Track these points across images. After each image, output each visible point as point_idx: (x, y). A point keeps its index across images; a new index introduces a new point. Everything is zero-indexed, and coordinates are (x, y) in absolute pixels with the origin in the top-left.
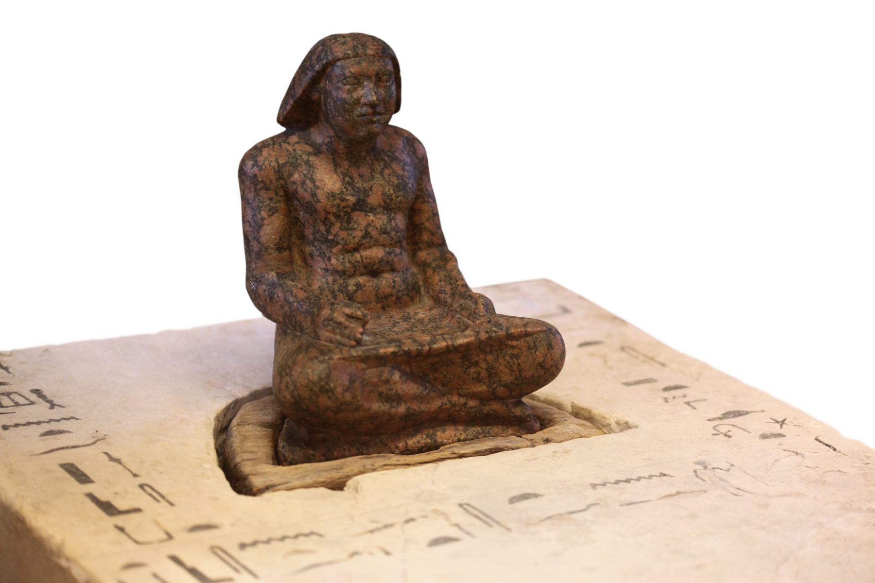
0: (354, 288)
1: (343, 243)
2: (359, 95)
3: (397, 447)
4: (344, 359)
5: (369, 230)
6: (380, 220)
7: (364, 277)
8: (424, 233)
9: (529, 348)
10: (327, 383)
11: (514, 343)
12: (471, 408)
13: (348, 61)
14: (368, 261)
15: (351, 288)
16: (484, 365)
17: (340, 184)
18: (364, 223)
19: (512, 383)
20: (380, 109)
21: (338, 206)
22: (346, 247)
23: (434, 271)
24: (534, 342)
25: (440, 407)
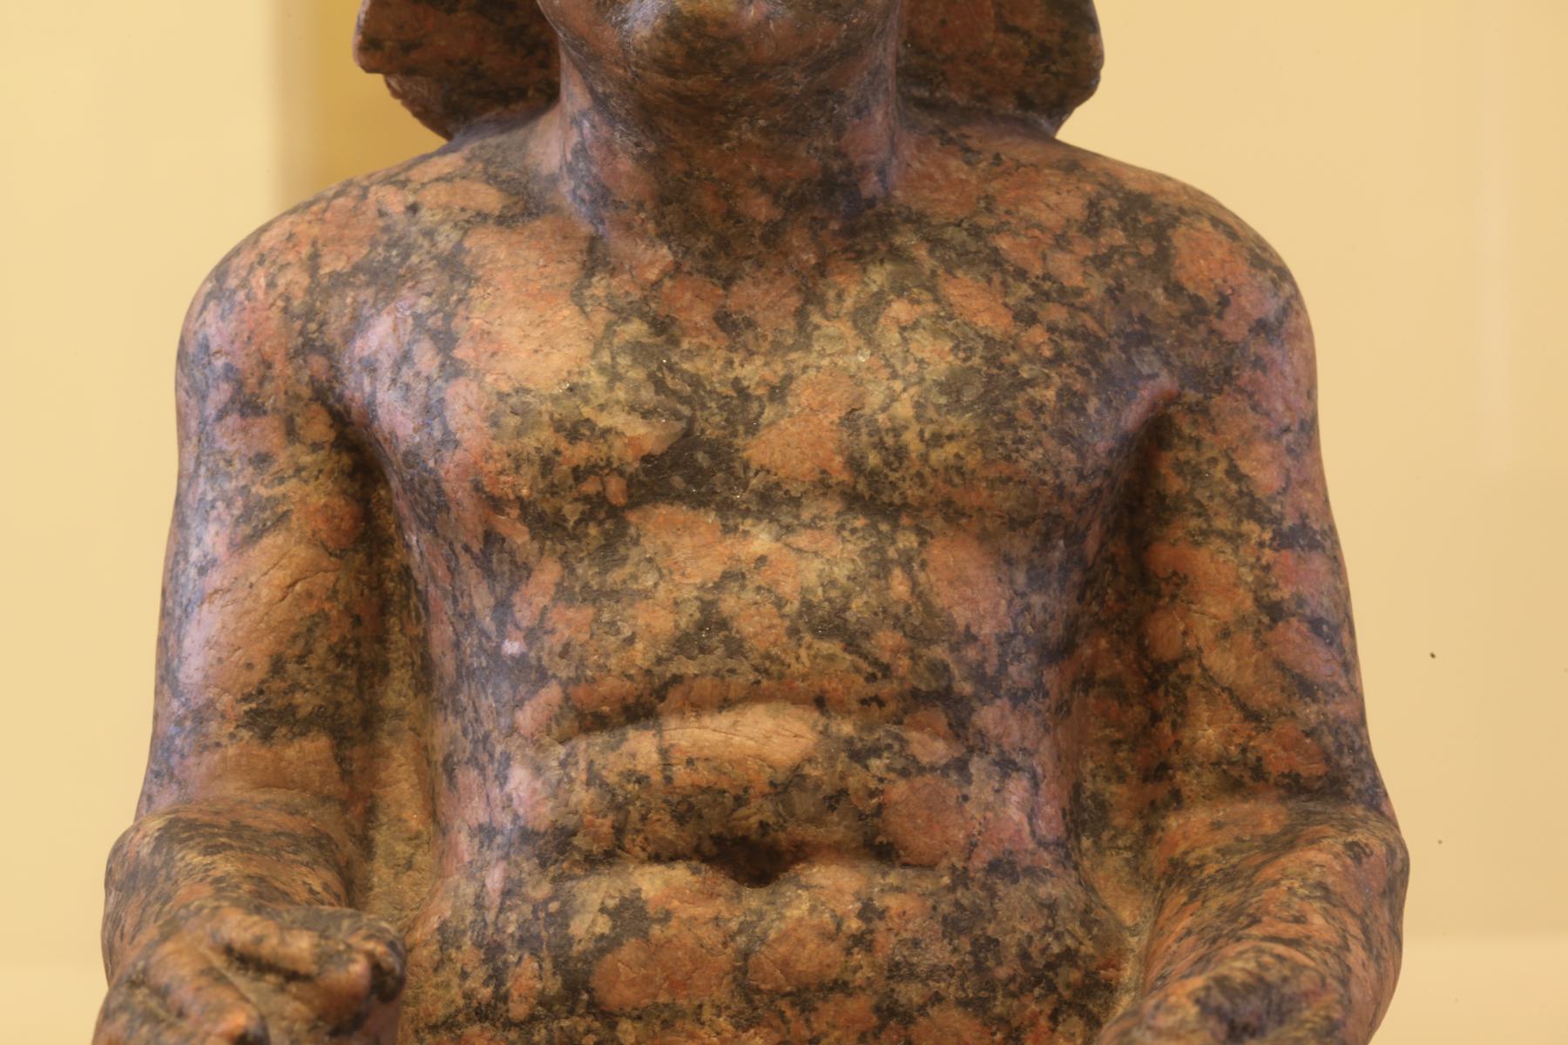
0: (603, 926)
1: (563, 674)
5: (729, 604)
6: (815, 559)
7: (680, 874)
8: (1202, 711)
14: (704, 776)
15: (588, 924)
17: (587, 348)
18: (710, 568)
21: (547, 464)
22: (580, 692)
23: (1193, 897)
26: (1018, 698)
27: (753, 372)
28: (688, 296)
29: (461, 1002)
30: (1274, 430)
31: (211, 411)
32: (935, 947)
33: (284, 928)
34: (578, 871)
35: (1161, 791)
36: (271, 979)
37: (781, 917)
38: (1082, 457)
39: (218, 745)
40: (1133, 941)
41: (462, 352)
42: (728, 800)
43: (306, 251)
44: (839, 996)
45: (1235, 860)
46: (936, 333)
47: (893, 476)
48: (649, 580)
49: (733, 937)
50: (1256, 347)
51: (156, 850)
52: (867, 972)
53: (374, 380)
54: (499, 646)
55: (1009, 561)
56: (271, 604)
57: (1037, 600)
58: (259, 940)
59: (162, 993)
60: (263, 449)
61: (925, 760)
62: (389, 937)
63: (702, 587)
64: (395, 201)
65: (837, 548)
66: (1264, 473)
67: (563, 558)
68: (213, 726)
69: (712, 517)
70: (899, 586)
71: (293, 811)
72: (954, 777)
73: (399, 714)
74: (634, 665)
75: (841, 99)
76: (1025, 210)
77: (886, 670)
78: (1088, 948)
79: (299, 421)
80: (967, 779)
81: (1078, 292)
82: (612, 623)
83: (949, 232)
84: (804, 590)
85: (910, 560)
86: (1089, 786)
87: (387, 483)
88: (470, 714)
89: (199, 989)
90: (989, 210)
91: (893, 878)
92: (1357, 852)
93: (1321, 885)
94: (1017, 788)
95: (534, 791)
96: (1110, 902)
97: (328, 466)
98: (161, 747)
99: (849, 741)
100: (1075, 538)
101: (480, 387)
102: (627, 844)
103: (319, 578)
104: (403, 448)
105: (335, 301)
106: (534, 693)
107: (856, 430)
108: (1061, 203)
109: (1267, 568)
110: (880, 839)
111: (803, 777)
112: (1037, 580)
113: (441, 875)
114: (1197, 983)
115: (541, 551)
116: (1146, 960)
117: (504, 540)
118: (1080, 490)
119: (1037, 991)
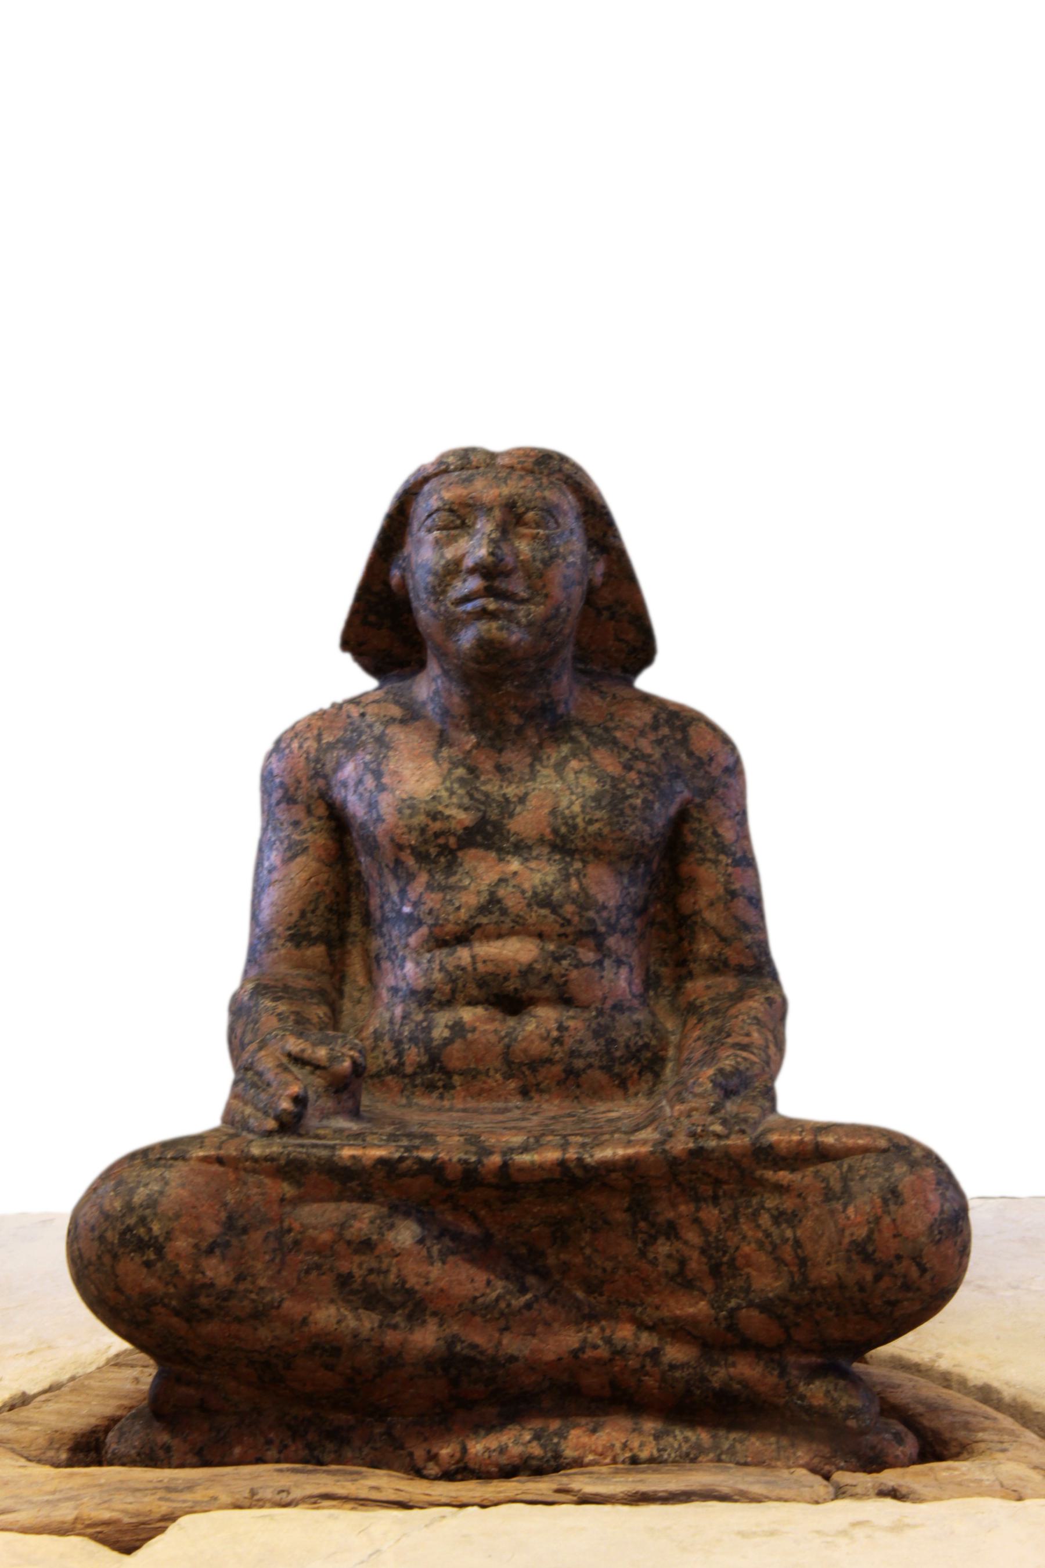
1: (430, 922)
2: (460, 553)
3: (433, 1457)
4: (220, 1161)
5: (501, 892)
6: (537, 873)
7: (480, 1011)
8: (702, 937)
9: (829, 1196)
10: (143, 1221)
11: (784, 1176)
12: (672, 1367)
13: (444, 478)
14: (490, 968)
15: (439, 1033)
16: (693, 1236)
17: (440, 780)
18: (492, 877)
19: (784, 1300)
20: (518, 586)
21: (423, 830)
22: (437, 930)
23: (700, 1020)
24: (845, 1179)
25: (575, 1354)
26: (624, 933)
27: (511, 791)
28: (483, 757)
29: (383, 1066)
30: (732, 814)
31: (274, 801)
32: (589, 1043)
33: (314, 1045)
34: (435, 1009)
35: (684, 971)
36: (308, 1068)
37: (523, 1030)
38: (652, 829)
39: (276, 949)
40: (673, 1038)
41: (386, 780)
42: (501, 978)
43: (315, 732)
44: (548, 1065)
45: (717, 1004)
46: (590, 775)
47: (572, 837)
48: (467, 882)
49: (503, 1038)
50: (725, 779)
51: (250, 999)
52: (560, 1055)
53: (346, 791)
54: (400, 910)
55: (621, 874)
56: (300, 888)
57: (632, 890)
58: (303, 1051)
59: (260, 1074)
60: (297, 818)
61: (585, 961)
62: (359, 1048)
63: (489, 885)
64: (355, 712)
65: (548, 868)
66: (729, 835)
67: (429, 871)
68: (274, 941)
69: (494, 854)
70: (574, 885)
71: (309, 979)
72: (597, 968)
73: (355, 935)
74: (459, 918)
75: (550, 673)
76: (627, 719)
77: (569, 922)
78: (654, 1042)
79: (313, 807)
80: (603, 969)
81: (650, 756)
82: (451, 901)
83: (595, 729)
84: (534, 887)
85: (579, 873)
86: (652, 968)
87: (350, 834)
88: (387, 938)
89: (277, 1074)
90: (612, 719)
91: (571, 1013)
92: (770, 1001)
93: (756, 1018)
94: (624, 972)
95: (416, 973)
96: (662, 1020)
97: (325, 827)
98: (252, 950)
99: (553, 953)
100: (648, 863)
101: (394, 796)
102: (457, 996)
103: (321, 875)
104: (359, 821)
105: (329, 755)
106: (416, 930)
107: (556, 817)
108: (643, 716)
109: (730, 875)
110: (566, 996)
111: (533, 969)
112: (632, 882)
113: (374, 1007)
114: (711, 1072)
115: (420, 868)
116: (679, 1048)
117: (403, 863)
118: (651, 843)
119: (633, 1062)
